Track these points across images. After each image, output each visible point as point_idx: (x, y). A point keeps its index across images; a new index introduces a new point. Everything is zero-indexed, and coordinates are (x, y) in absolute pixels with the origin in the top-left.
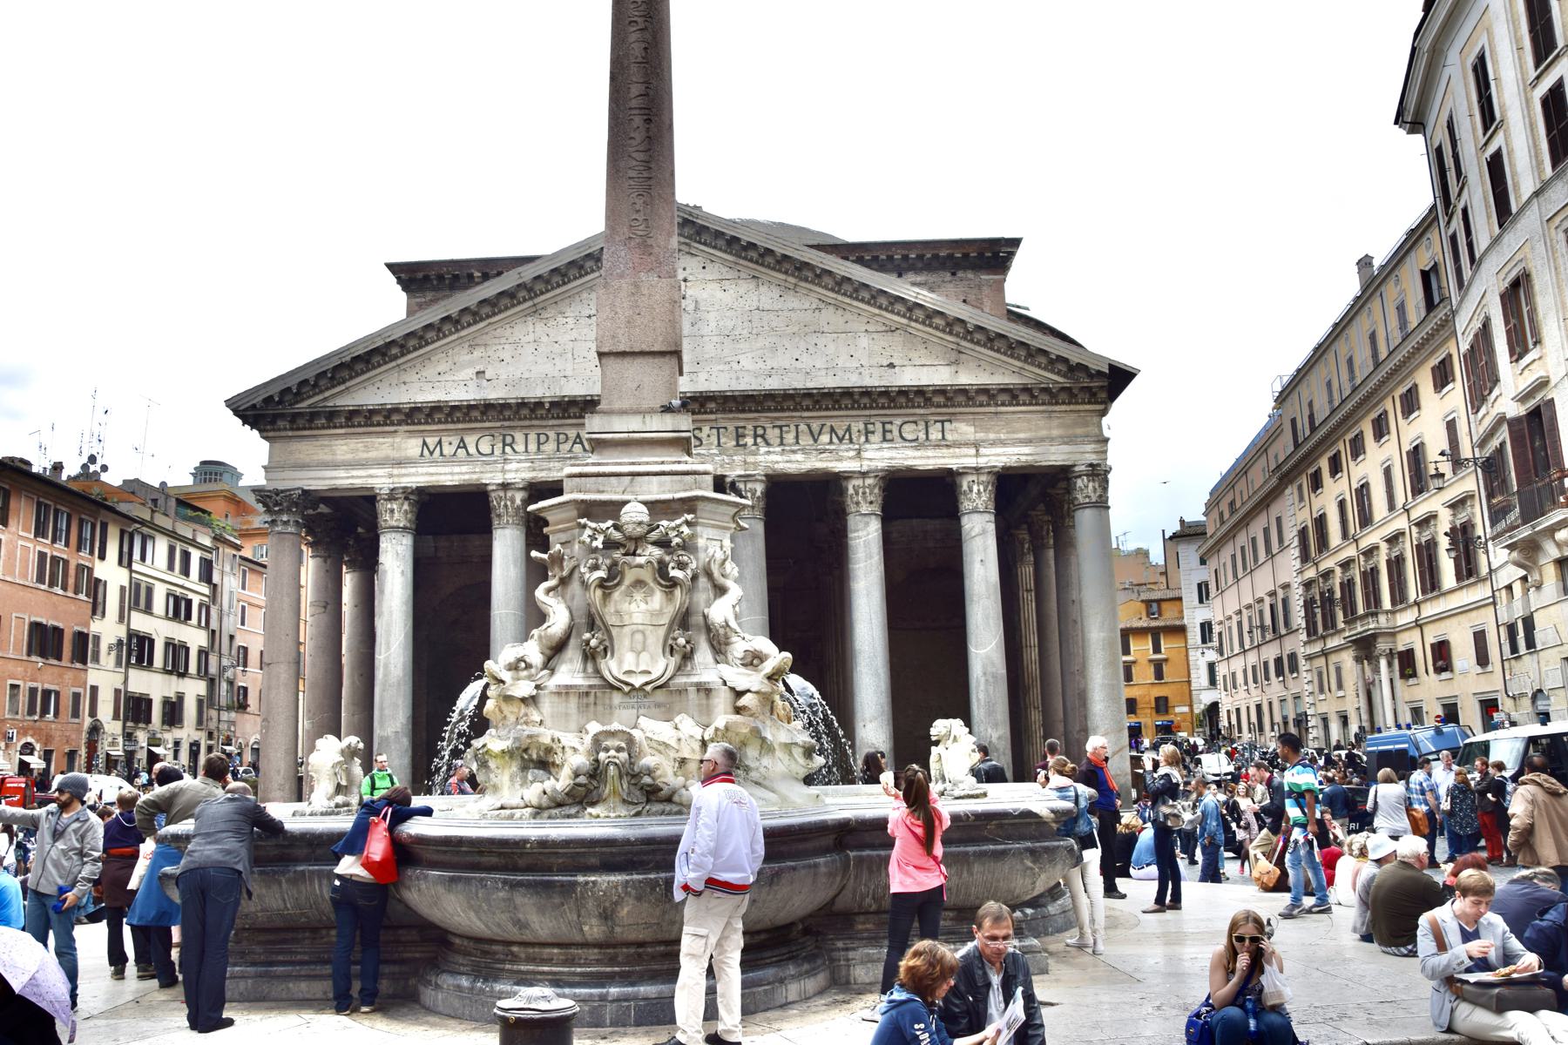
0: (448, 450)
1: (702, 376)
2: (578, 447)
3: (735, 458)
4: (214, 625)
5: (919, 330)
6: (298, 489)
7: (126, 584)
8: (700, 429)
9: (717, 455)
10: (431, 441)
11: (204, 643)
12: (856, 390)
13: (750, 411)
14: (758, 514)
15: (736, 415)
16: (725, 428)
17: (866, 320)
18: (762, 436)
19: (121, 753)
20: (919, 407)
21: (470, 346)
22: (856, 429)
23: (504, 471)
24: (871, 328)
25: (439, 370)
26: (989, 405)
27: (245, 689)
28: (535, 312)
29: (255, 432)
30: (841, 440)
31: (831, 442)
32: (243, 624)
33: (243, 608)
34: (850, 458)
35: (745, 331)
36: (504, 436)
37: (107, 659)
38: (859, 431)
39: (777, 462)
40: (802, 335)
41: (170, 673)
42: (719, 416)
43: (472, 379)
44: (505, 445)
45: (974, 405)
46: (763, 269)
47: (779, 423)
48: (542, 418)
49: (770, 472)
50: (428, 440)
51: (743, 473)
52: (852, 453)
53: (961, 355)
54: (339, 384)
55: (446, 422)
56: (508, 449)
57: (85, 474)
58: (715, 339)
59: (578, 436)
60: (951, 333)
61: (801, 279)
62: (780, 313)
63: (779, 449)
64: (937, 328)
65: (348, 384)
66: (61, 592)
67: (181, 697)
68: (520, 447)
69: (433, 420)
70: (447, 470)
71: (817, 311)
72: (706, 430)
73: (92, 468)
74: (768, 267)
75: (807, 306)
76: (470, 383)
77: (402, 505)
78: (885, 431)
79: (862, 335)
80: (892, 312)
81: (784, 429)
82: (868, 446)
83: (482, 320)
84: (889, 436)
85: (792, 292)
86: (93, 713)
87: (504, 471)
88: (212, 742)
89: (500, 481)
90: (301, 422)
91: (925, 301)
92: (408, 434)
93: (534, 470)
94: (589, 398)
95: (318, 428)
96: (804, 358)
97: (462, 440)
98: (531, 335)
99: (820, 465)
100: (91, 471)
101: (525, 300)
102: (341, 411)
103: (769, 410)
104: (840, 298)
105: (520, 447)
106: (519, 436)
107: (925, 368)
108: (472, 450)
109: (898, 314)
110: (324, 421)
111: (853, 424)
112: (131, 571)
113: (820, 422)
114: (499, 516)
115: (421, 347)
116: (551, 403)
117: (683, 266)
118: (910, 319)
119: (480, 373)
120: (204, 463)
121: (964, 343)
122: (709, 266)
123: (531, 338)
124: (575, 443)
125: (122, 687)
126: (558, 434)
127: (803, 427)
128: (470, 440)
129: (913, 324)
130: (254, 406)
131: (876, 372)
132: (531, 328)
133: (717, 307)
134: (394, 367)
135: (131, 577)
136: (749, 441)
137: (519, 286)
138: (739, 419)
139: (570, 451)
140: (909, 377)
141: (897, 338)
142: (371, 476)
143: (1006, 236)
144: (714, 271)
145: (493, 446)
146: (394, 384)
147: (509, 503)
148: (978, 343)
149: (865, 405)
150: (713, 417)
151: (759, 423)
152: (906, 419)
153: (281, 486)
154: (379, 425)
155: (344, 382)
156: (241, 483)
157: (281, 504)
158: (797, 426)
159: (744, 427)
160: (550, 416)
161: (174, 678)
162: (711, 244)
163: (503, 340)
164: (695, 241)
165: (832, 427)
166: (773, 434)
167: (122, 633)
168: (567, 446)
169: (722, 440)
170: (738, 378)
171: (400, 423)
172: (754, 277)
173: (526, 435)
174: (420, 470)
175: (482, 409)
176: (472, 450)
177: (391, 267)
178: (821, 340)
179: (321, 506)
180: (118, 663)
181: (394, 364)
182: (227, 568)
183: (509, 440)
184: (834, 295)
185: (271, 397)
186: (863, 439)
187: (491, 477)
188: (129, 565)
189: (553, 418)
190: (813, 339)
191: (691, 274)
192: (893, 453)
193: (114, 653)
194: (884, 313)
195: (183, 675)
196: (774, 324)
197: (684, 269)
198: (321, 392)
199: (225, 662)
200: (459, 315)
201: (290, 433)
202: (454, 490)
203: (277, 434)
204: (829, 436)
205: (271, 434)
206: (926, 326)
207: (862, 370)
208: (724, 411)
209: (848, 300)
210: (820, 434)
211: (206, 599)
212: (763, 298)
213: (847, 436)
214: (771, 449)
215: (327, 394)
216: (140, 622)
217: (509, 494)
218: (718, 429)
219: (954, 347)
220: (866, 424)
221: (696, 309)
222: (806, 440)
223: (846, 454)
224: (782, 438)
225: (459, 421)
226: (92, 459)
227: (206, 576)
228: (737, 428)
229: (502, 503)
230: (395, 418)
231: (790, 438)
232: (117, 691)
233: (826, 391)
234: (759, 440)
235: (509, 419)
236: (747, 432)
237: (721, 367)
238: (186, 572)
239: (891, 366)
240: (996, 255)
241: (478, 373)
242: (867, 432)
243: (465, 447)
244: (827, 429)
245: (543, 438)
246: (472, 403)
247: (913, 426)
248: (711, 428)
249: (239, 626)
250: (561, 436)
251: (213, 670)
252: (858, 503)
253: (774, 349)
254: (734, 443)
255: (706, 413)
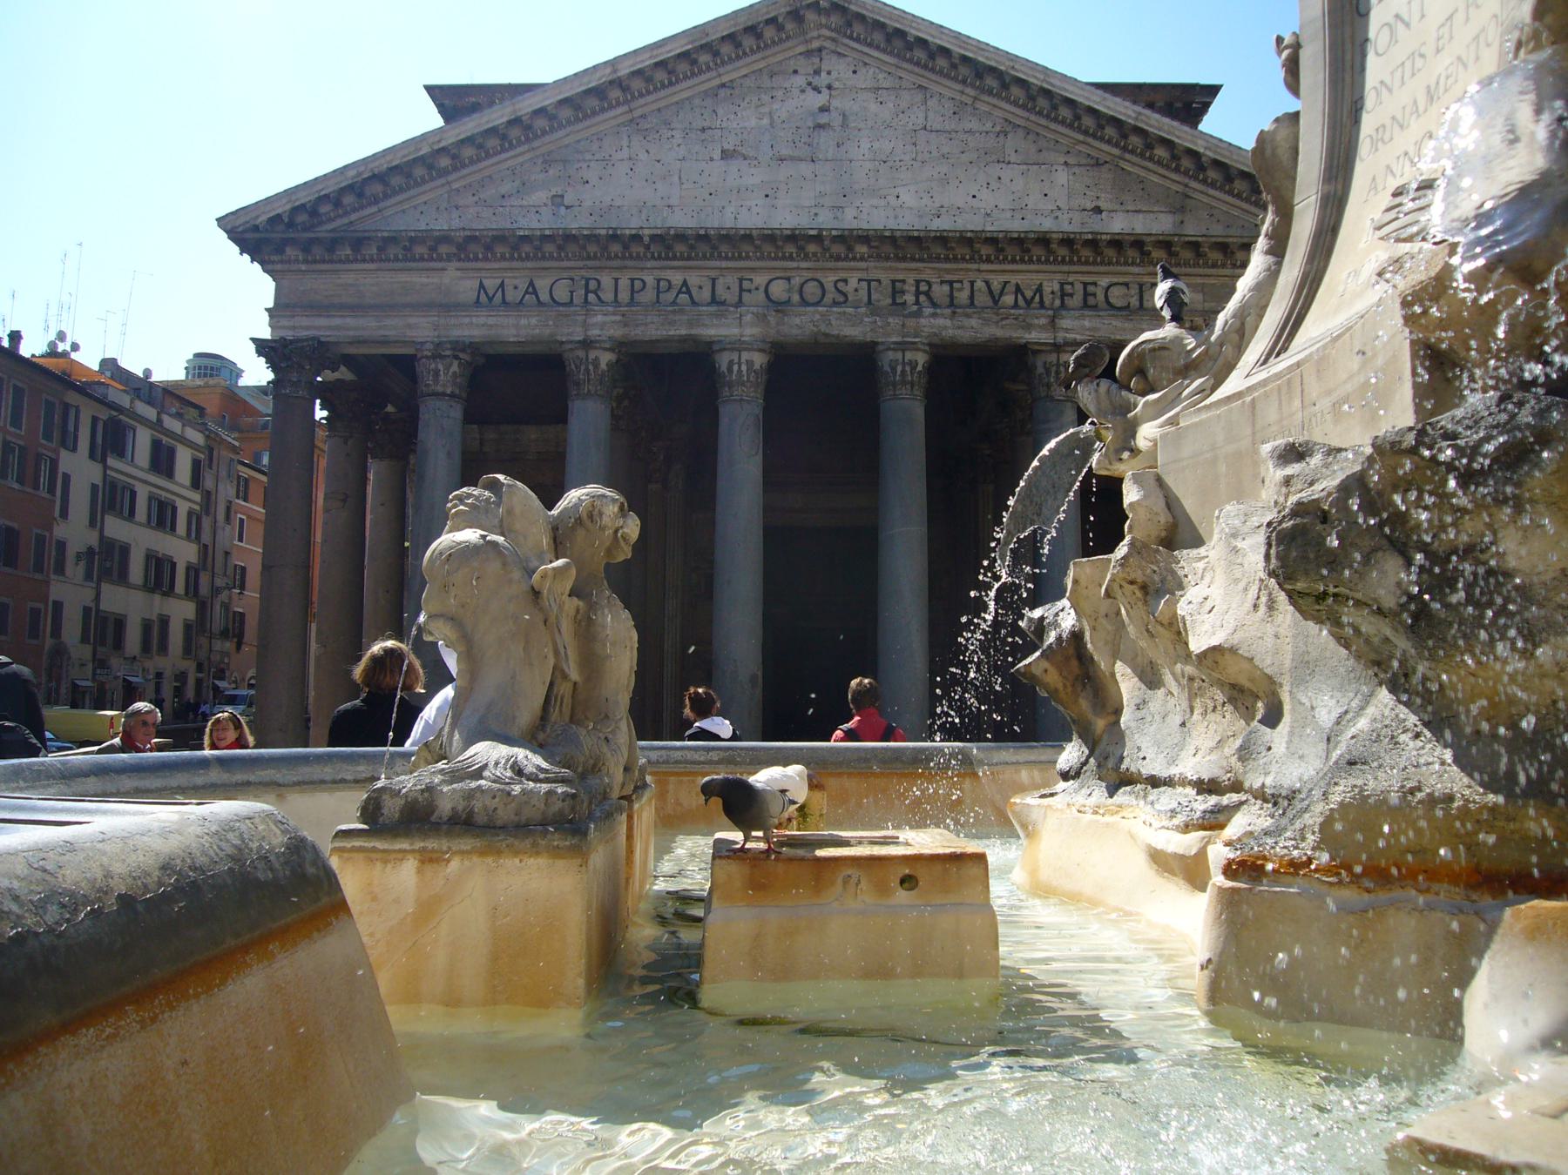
0: (511, 296)
1: (850, 213)
2: (684, 297)
3: (890, 320)
4: (206, 537)
5: (1134, 164)
6: (313, 338)
7: (98, 481)
8: (845, 281)
9: (867, 316)
10: (491, 284)
11: (194, 559)
12: (1054, 236)
13: (913, 259)
14: (918, 392)
15: (893, 264)
16: (879, 281)
17: (1066, 149)
18: (927, 294)
19: (89, 684)
20: (1133, 264)
21: (545, 162)
22: (1049, 290)
23: (585, 325)
24: (1071, 161)
25: (503, 192)
26: (1224, 266)
27: (242, 615)
28: (631, 121)
29: (257, 266)
30: (1029, 302)
31: (1016, 306)
32: (241, 540)
33: (242, 521)
34: (1042, 328)
35: (907, 158)
36: (587, 280)
37: (75, 571)
38: (1053, 293)
39: (946, 328)
40: (982, 165)
41: (152, 591)
42: (872, 264)
43: (545, 205)
44: (587, 291)
45: (1206, 265)
46: (933, 77)
47: (948, 277)
48: (638, 257)
49: (936, 340)
50: (486, 282)
51: (899, 339)
52: (1043, 321)
53: (1188, 201)
54: (370, 204)
55: (512, 258)
56: (591, 297)
57: (53, 353)
58: (868, 165)
59: (685, 283)
60: (1177, 170)
61: (982, 90)
62: (954, 135)
63: (948, 311)
64: (1159, 163)
65: (382, 205)
66: (16, 486)
67: (164, 621)
68: (608, 296)
69: (494, 255)
70: (511, 321)
71: (1002, 136)
72: (853, 283)
73: (61, 347)
74: (941, 73)
75: (989, 126)
76: (543, 210)
77: (451, 365)
78: (1086, 294)
79: (1060, 168)
80: (1102, 139)
81: (955, 285)
82: (1064, 313)
83: (561, 126)
84: (1091, 301)
85: (969, 109)
86: (57, 631)
87: (585, 325)
88: (201, 675)
89: (580, 338)
90: (318, 251)
91: (1147, 124)
92: (459, 273)
93: (626, 325)
94: (702, 232)
95: (340, 261)
96: (985, 194)
97: (531, 284)
98: (625, 149)
99: (1000, 333)
100: (60, 350)
101: (619, 104)
102: (369, 238)
103: (938, 259)
104: (1033, 117)
105: (608, 296)
106: (607, 280)
107: (1141, 216)
108: (545, 297)
109: (1109, 142)
110: (349, 252)
111: (1045, 284)
112: (106, 467)
113: (1006, 277)
114: (578, 384)
115: (479, 160)
116: (653, 238)
117: (827, 68)
118: (1125, 149)
119: (557, 200)
120: (198, 355)
121: (1194, 184)
122: (862, 71)
123: (625, 154)
124: (680, 292)
125: (92, 605)
126: (659, 281)
127: (979, 284)
128: (542, 284)
129: (1128, 156)
130: (256, 228)
131: (1077, 217)
132: (626, 138)
133: (870, 123)
134: (443, 185)
135: (105, 475)
136: (910, 298)
137: (611, 82)
138: (897, 269)
139: (674, 303)
140: (1117, 224)
141: (1106, 174)
142: (410, 326)
143: (1203, 82)
144: (865, 78)
145: (572, 292)
146: (442, 208)
147: (591, 367)
148: (1213, 185)
149: (1064, 258)
150: (863, 265)
151: (923, 277)
152: (1115, 280)
153: (289, 335)
154: (422, 259)
155: (376, 201)
156: (242, 382)
157: (290, 359)
158: (972, 283)
159: (903, 281)
160: (649, 255)
161: (157, 597)
162: (866, 39)
163: (588, 156)
164: (845, 35)
165: (1017, 285)
166: (940, 291)
167: (92, 539)
168: (670, 296)
169: (874, 297)
170: (896, 217)
171: (449, 258)
172: (920, 86)
173: (616, 280)
174: (474, 320)
175: (560, 242)
176: (545, 297)
177: (430, 89)
178: (1007, 173)
179: (343, 368)
180: (88, 576)
181: (443, 181)
182: (223, 473)
183: (593, 285)
184: (1026, 114)
185: (279, 216)
186: (1058, 303)
187: (571, 332)
188: (104, 461)
189: (653, 257)
190: (995, 170)
191: (837, 79)
192: (1096, 323)
193: (82, 564)
194: (1090, 140)
195: (169, 592)
196: (945, 150)
197: (829, 73)
198: (346, 214)
199: (219, 582)
200: (531, 118)
201: (303, 267)
202: (519, 350)
203: (286, 267)
204: (1013, 297)
205: (279, 267)
206: (1145, 159)
207: (1059, 213)
208: (879, 257)
209: (1043, 122)
210: (1002, 293)
211: (197, 508)
212: (931, 115)
213: (1037, 298)
214: (938, 311)
215: (353, 217)
216: (116, 528)
217: (592, 355)
218: (869, 282)
219: (1180, 188)
220: (1062, 285)
221: (844, 125)
222: (982, 299)
223: (1036, 321)
224: (951, 297)
225: (528, 258)
226: (61, 336)
227: (196, 483)
228: (894, 282)
229: (583, 368)
230: (444, 249)
231: (963, 296)
232: (87, 610)
233: (1016, 235)
234: (922, 298)
235: (595, 258)
236: (906, 287)
237: (875, 202)
238: (169, 473)
239: (1098, 210)
240: (1188, 106)
241: (554, 196)
242: (1063, 295)
243: (535, 293)
244: (1010, 288)
245: (638, 284)
246: (547, 233)
247: (1123, 290)
248: (860, 280)
249: (236, 542)
250: (662, 283)
251: (204, 590)
252: (1049, 386)
253: (945, 181)
254: (890, 301)
255: (854, 259)
